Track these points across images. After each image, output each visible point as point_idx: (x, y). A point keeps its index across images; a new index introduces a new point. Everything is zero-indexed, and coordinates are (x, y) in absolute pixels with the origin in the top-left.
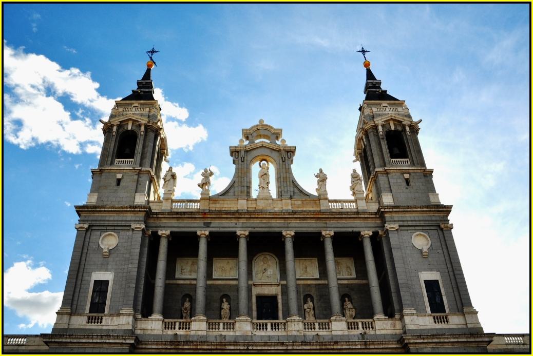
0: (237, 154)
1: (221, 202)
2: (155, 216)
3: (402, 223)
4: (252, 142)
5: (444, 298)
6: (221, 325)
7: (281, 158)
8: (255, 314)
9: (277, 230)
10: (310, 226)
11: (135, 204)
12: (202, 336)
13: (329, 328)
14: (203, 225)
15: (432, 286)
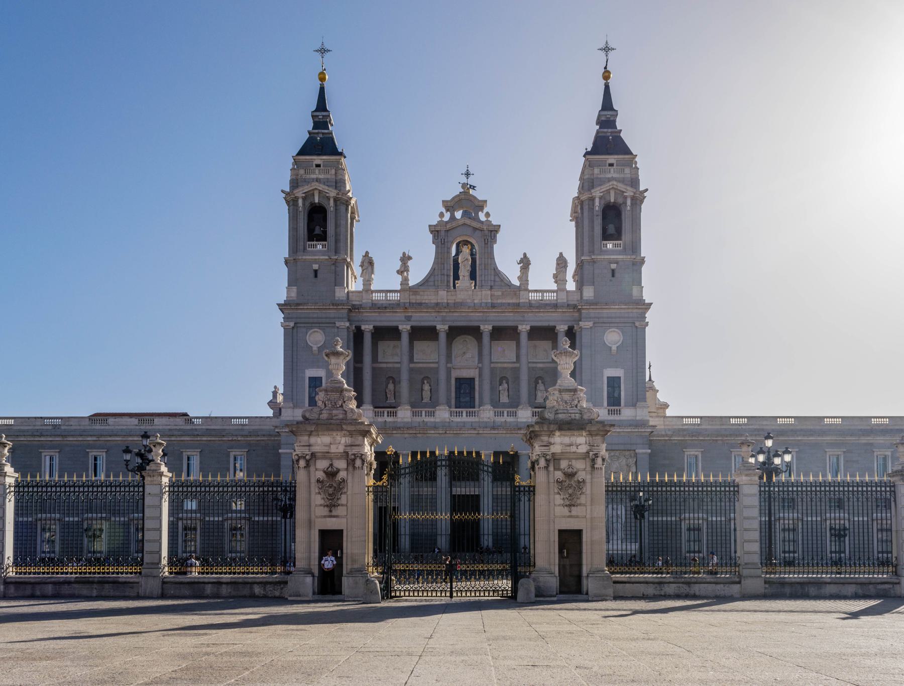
0: (436, 233)
1: (421, 293)
2: (357, 310)
3: (597, 320)
4: (453, 218)
5: (623, 393)
6: (424, 413)
7: (483, 240)
8: (453, 402)
9: (476, 324)
10: (506, 319)
11: (336, 298)
12: (408, 423)
13: (516, 415)
14: (403, 319)
15: (614, 383)
